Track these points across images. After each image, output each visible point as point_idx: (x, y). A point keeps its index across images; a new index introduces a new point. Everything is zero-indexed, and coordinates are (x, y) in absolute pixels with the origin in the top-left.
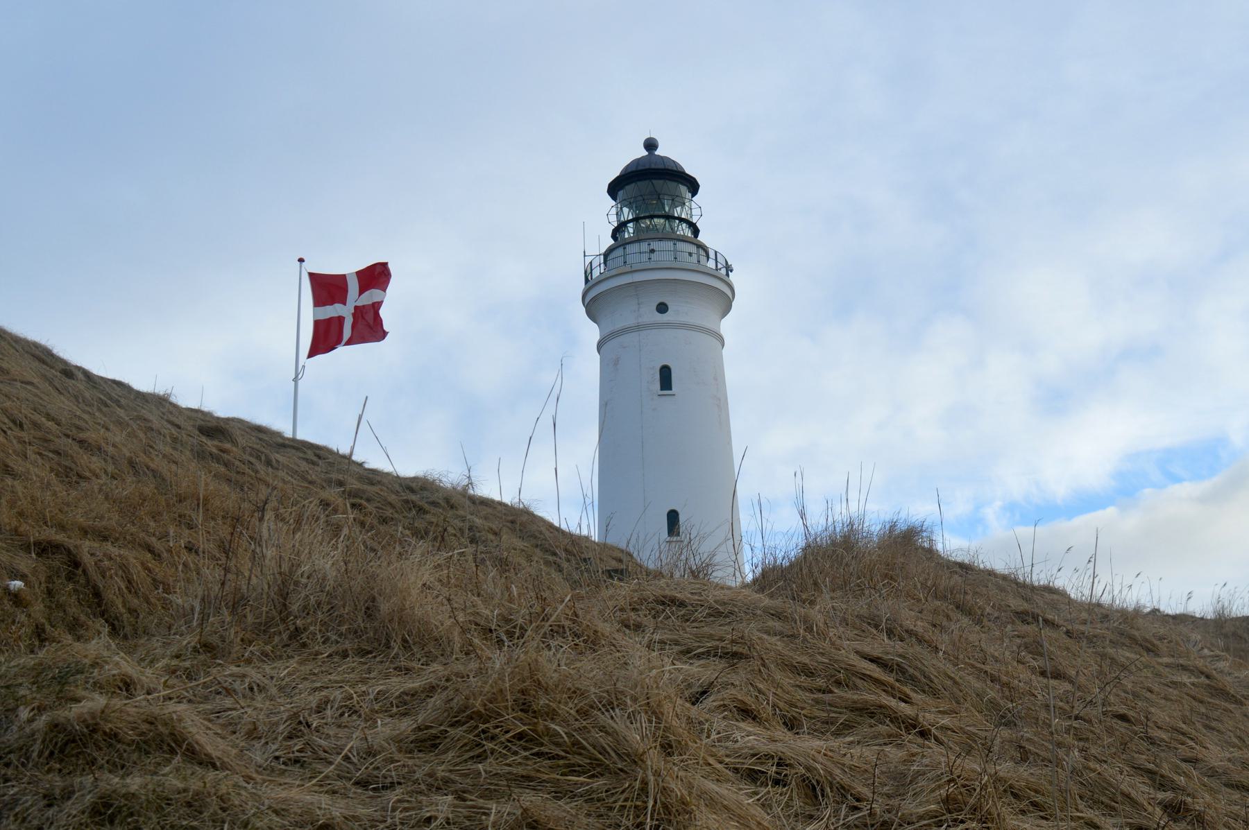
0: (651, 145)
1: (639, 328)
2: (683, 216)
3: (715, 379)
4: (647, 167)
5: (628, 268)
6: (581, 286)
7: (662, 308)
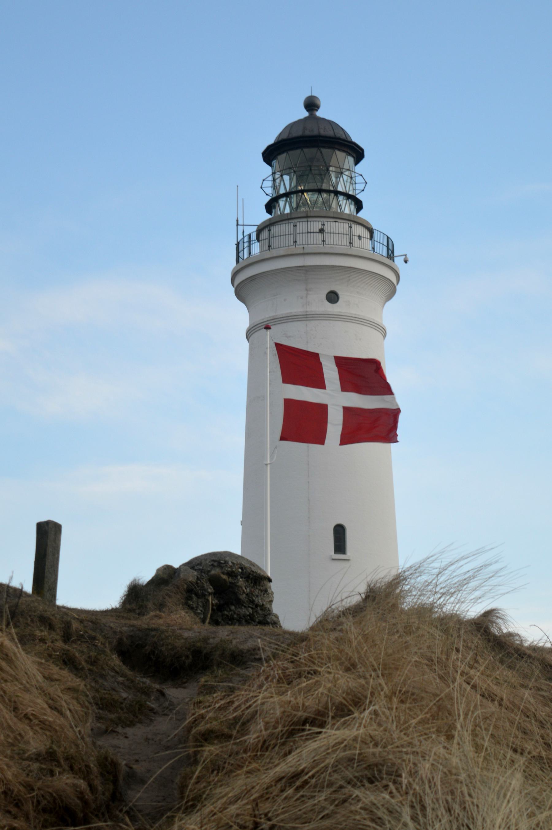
1: (306, 317)
2: (351, 193)
4: (315, 133)
7: (333, 297)
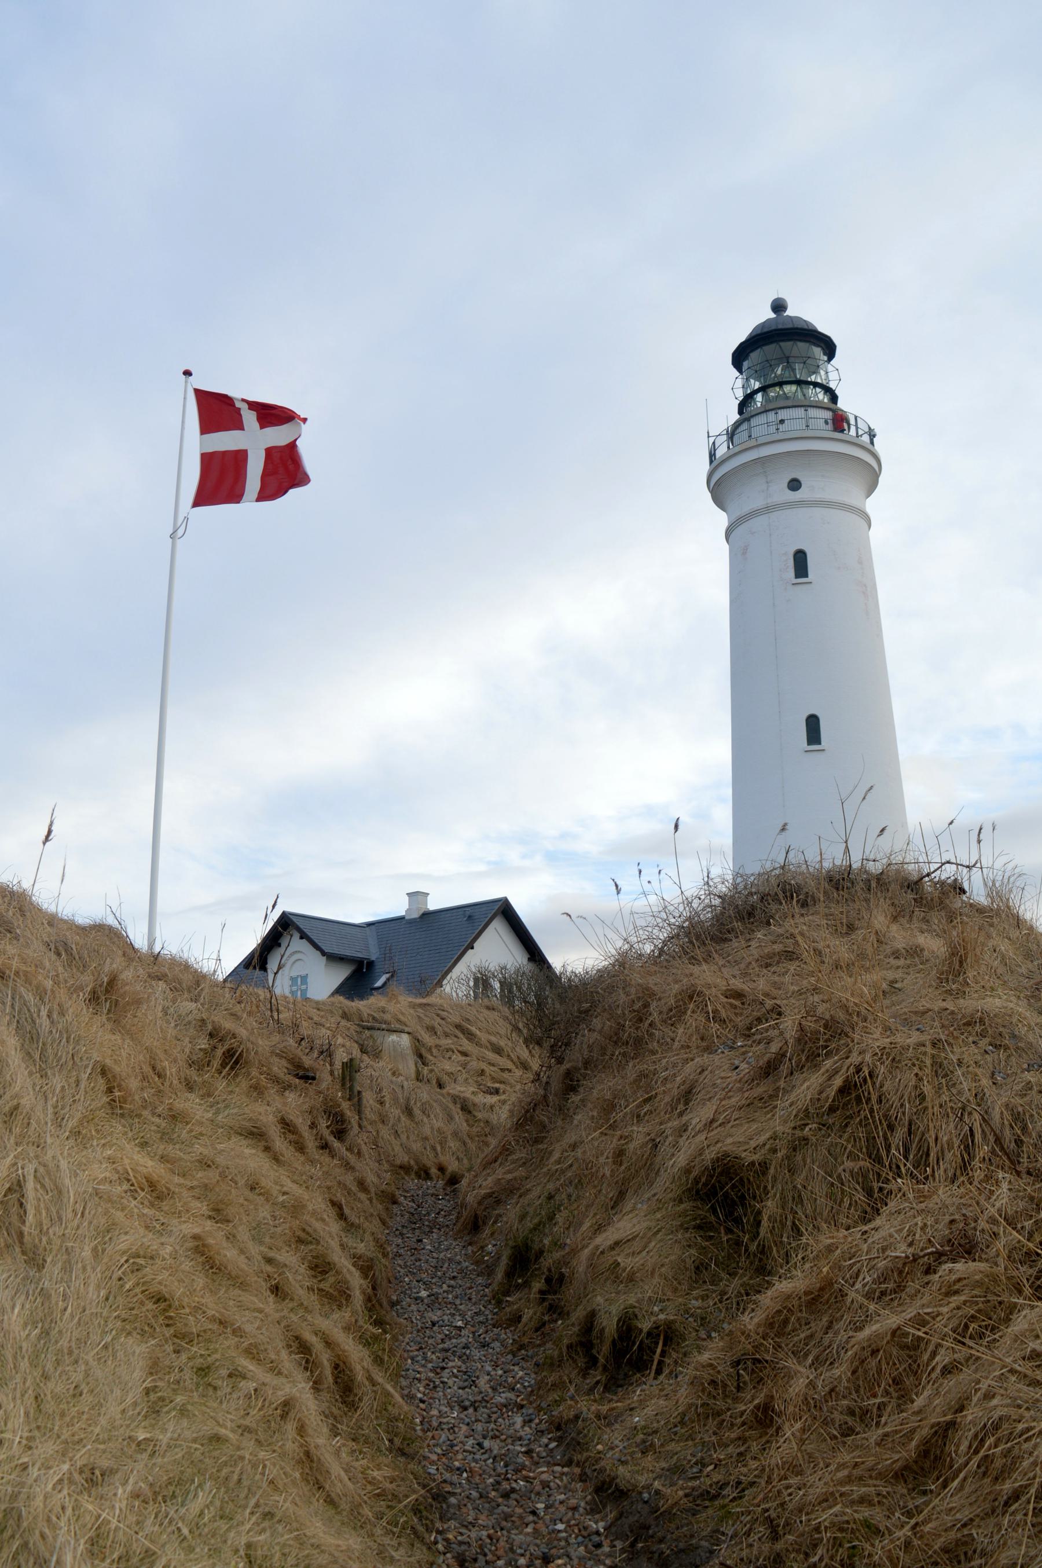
0: (779, 306)
1: (768, 509)
3: (860, 562)
4: (773, 328)
5: (753, 443)
6: (705, 467)
7: (795, 485)
